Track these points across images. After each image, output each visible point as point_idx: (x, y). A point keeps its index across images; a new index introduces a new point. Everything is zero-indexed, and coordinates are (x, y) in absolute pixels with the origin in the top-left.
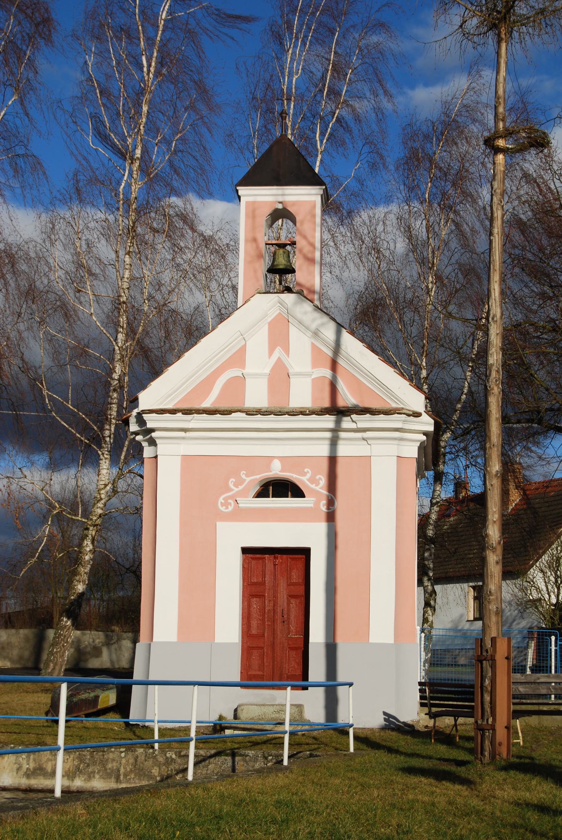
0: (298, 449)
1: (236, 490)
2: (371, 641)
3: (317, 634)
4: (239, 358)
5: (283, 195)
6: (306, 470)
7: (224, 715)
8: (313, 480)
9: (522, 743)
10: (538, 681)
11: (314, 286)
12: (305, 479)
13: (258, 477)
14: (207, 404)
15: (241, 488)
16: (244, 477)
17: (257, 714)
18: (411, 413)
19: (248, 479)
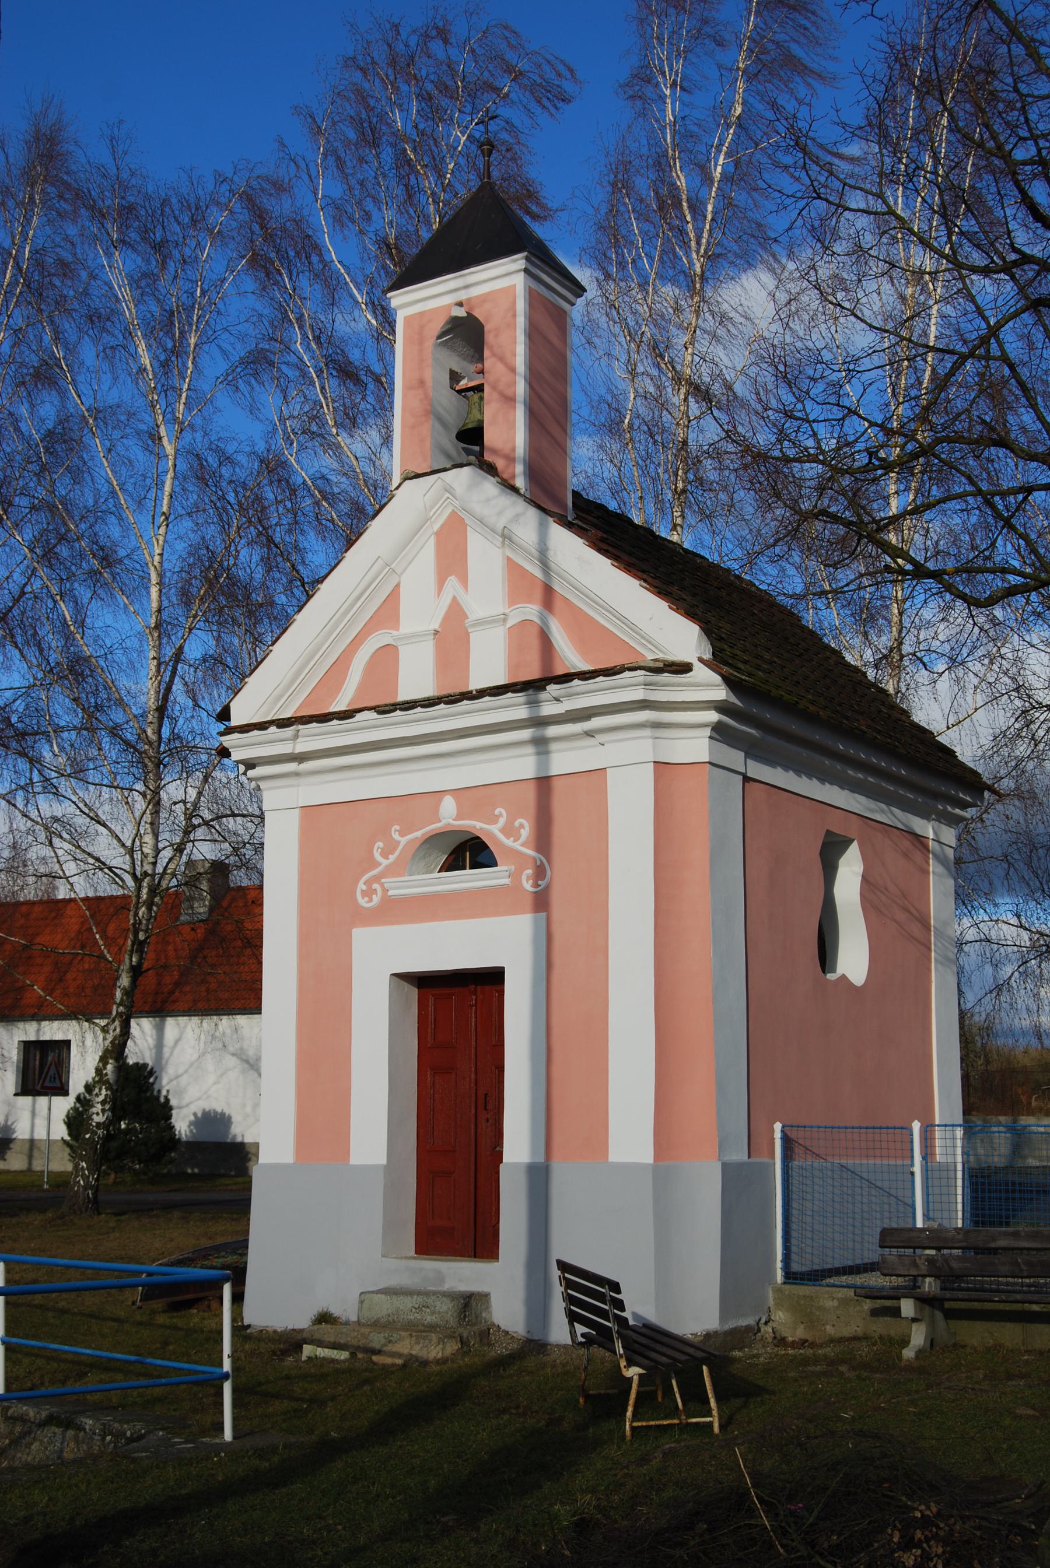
0: (475, 772)
1: (385, 863)
2: (612, 1158)
3: (518, 1146)
4: (388, 612)
5: (466, 287)
6: (497, 812)
7: (336, 1311)
8: (510, 830)
9: (716, 1429)
10: (993, 1245)
11: (514, 449)
12: (495, 829)
13: (419, 834)
14: (340, 705)
15: (392, 858)
16: (396, 836)
17: (385, 1312)
18: (661, 665)
19: (403, 840)
